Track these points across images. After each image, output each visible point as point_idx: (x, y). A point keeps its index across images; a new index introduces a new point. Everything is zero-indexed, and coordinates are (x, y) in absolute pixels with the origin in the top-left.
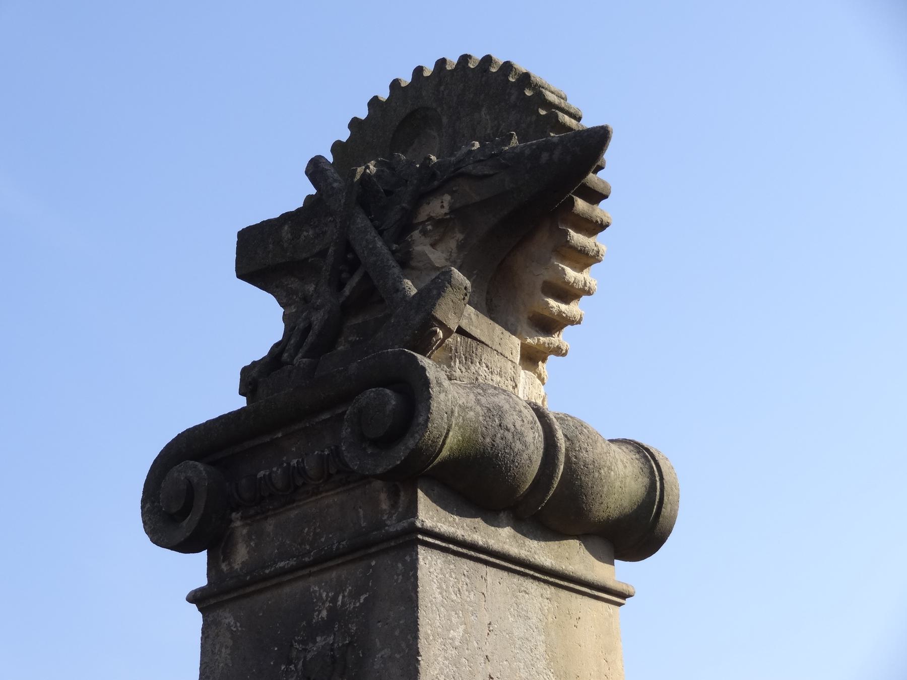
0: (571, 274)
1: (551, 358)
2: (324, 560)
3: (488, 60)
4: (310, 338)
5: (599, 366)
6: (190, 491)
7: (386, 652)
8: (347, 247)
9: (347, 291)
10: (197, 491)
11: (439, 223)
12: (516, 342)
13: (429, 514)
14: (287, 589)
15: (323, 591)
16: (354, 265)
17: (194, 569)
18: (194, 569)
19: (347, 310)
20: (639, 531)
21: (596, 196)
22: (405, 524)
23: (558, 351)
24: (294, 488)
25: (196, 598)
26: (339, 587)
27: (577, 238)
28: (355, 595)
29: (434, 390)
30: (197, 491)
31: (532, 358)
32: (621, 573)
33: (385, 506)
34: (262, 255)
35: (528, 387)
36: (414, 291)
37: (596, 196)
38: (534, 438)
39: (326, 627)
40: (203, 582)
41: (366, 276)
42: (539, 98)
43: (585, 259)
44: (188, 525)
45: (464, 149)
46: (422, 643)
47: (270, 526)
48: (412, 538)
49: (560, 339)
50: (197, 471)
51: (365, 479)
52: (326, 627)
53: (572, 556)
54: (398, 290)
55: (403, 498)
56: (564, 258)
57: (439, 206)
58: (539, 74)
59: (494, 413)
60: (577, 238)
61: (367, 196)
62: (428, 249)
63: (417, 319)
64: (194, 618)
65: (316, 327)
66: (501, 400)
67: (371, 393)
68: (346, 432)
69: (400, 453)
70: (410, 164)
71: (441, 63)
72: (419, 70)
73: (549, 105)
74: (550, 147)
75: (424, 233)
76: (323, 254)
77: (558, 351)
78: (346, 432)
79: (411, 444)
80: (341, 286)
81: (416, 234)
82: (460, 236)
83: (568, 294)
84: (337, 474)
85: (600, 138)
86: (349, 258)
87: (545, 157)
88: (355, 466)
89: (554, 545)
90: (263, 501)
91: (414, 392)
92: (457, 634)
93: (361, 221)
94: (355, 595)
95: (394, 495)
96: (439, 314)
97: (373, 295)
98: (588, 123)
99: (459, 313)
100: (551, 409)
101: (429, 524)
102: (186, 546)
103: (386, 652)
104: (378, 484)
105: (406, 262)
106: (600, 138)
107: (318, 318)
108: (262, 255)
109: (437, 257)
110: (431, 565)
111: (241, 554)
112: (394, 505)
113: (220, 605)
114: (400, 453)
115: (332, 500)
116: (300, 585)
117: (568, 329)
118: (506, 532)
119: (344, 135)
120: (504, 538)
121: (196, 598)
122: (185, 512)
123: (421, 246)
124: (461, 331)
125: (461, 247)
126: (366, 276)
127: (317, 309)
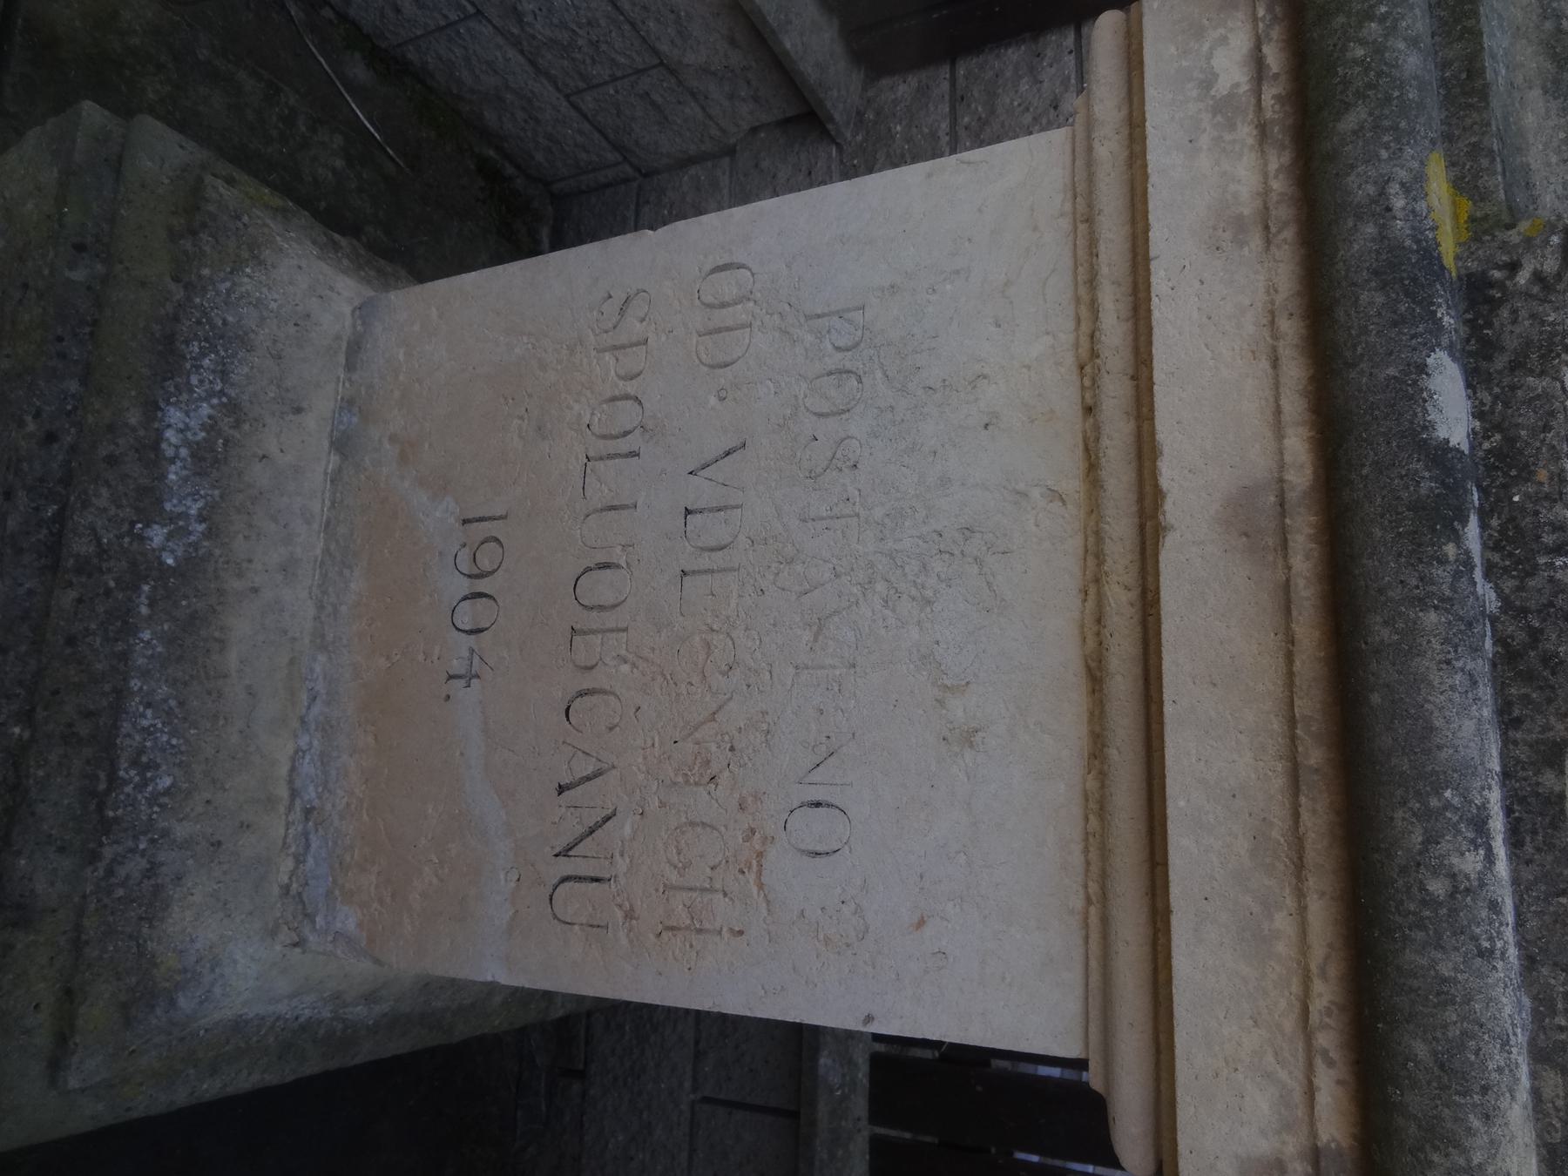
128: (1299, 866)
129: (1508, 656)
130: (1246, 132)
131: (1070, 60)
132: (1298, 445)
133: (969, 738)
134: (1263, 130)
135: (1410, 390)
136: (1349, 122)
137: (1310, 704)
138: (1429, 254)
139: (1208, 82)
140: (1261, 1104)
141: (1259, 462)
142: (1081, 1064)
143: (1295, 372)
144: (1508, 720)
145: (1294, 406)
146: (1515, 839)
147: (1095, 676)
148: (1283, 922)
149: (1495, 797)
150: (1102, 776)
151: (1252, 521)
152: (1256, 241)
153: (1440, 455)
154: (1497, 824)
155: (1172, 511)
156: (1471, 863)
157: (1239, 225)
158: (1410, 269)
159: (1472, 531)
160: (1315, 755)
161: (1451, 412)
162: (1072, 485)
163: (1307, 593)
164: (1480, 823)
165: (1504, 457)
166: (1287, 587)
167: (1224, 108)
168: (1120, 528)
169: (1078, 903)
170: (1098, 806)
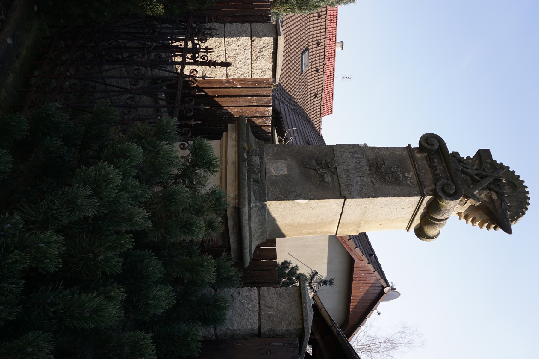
0: (477, 223)
1: (458, 217)
2: (418, 175)
3: (529, 204)
4: (465, 169)
5: (456, 222)
6: (433, 145)
7: (399, 190)
8: (486, 176)
9: (476, 177)
10: (432, 145)
11: (491, 197)
12: (463, 211)
13: (427, 198)
14: (411, 166)
15: (411, 175)
16: (482, 178)
17: (415, 145)
18: (415, 145)
19: (472, 177)
20: (420, 233)
21: (495, 228)
22: (425, 194)
23: (460, 219)
24: (433, 168)
25: (409, 146)
26: (412, 179)
27: (486, 225)
28: (410, 182)
29: (454, 201)
30: (432, 145)
31: (459, 214)
32: (412, 229)
33: (429, 188)
34: (484, 155)
35: (453, 217)
36: (475, 193)
37: (495, 228)
38: (443, 218)
39: (404, 176)
40: (412, 147)
41: (479, 181)
42: (519, 217)
43: (481, 226)
44: (425, 144)
45: (508, 202)
46: (401, 198)
47: (424, 162)
48: (423, 195)
49: (463, 220)
50: (436, 146)
51: (435, 184)
52: (404, 176)
53: (417, 221)
54: (476, 190)
55: (431, 193)
56: (481, 221)
57: (494, 196)
58: (524, 216)
59: (448, 211)
60: (486, 225)
61: (497, 181)
62: (485, 194)
63: (469, 195)
64: (405, 146)
65: (468, 171)
66: (451, 212)
67: (454, 187)
68: (445, 181)
69: (441, 194)
70: (505, 190)
71: (528, 193)
72: (526, 187)
73: (517, 219)
74: (508, 221)
75: (488, 193)
76: (484, 170)
77: (460, 219)
78: (445, 181)
79: (443, 196)
80: (477, 175)
81: (488, 191)
82: (487, 201)
83: (473, 222)
84: (436, 180)
85: (509, 231)
86: (483, 177)
87: (505, 220)
88: (438, 184)
89: (419, 219)
90: (430, 160)
91: (454, 196)
92: (402, 203)
93: (492, 179)
94: (410, 182)
95: (431, 191)
96: (470, 199)
97: (475, 182)
98: (514, 226)
99: (470, 202)
100: (447, 220)
101: (425, 199)
102: (420, 143)
103: (399, 190)
104: (434, 187)
105: (483, 189)
106: (509, 231)
107: (470, 171)
108: (484, 155)
109: (483, 196)
110: (417, 198)
111: (418, 155)
112: (429, 191)
113: (408, 151)
114: (441, 194)
115: (430, 176)
116: (412, 170)
117: (465, 221)
118: (423, 211)
119: (511, 169)
120: (421, 210)
121: (409, 146)
122: (427, 143)
123: (485, 192)
124: (466, 203)
125: (485, 201)
126: (479, 181)
127: (472, 170)
132: (237, 159)
137: (237, 172)
140: (232, 195)
141: (234, 160)
143: (237, 154)
151: (233, 163)
167: (233, 139)
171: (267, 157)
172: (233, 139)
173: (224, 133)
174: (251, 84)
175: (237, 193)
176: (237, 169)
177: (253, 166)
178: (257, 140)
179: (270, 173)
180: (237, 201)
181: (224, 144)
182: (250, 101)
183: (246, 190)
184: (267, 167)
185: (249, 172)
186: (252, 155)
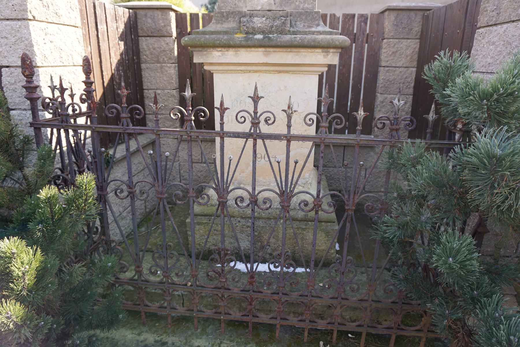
128: (299, 52)
129: (281, 34)
130: (226, 53)
131: (150, 91)
133: (286, 87)
134: (227, 51)
135: (258, 40)
136: (232, 43)
137: (284, 50)
138: (245, 37)
139: (220, 56)
140: (319, 56)
141: (261, 53)
142: (319, 75)
143: (253, 49)
144: (286, 34)
145: (256, 49)
146: (296, 35)
147: (280, 72)
148: (304, 53)
149: (293, 36)
150: (291, 71)
151: (266, 54)
152: (238, 52)
153: (264, 38)
154: (295, 36)
155: (265, 62)
156: (298, 38)
157: (236, 54)
158: (247, 39)
159: (270, 36)
160: (289, 50)
161: (259, 37)
162: (258, 74)
163: (274, 49)
164: (295, 37)
165: (263, 32)
166: (274, 51)
167: (223, 55)
168: (265, 68)
169: (303, 75)
170: (293, 72)
171: (242, 8)
172: (223, 55)
173: (206, 68)
174: (85, 30)
175: (320, 50)
176: (278, 50)
177: (272, 27)
178: (213, 21)
179: (270, 4)
180: (332, 50)
181: (221, 68)
182: (103, 35)
183: (309, 37)
184: (259, 8)
185: (282, 32)
186: (253, 28)
